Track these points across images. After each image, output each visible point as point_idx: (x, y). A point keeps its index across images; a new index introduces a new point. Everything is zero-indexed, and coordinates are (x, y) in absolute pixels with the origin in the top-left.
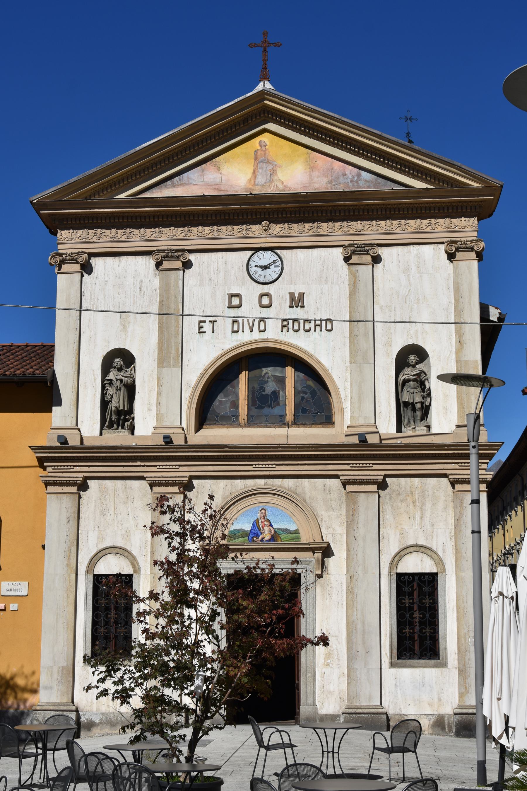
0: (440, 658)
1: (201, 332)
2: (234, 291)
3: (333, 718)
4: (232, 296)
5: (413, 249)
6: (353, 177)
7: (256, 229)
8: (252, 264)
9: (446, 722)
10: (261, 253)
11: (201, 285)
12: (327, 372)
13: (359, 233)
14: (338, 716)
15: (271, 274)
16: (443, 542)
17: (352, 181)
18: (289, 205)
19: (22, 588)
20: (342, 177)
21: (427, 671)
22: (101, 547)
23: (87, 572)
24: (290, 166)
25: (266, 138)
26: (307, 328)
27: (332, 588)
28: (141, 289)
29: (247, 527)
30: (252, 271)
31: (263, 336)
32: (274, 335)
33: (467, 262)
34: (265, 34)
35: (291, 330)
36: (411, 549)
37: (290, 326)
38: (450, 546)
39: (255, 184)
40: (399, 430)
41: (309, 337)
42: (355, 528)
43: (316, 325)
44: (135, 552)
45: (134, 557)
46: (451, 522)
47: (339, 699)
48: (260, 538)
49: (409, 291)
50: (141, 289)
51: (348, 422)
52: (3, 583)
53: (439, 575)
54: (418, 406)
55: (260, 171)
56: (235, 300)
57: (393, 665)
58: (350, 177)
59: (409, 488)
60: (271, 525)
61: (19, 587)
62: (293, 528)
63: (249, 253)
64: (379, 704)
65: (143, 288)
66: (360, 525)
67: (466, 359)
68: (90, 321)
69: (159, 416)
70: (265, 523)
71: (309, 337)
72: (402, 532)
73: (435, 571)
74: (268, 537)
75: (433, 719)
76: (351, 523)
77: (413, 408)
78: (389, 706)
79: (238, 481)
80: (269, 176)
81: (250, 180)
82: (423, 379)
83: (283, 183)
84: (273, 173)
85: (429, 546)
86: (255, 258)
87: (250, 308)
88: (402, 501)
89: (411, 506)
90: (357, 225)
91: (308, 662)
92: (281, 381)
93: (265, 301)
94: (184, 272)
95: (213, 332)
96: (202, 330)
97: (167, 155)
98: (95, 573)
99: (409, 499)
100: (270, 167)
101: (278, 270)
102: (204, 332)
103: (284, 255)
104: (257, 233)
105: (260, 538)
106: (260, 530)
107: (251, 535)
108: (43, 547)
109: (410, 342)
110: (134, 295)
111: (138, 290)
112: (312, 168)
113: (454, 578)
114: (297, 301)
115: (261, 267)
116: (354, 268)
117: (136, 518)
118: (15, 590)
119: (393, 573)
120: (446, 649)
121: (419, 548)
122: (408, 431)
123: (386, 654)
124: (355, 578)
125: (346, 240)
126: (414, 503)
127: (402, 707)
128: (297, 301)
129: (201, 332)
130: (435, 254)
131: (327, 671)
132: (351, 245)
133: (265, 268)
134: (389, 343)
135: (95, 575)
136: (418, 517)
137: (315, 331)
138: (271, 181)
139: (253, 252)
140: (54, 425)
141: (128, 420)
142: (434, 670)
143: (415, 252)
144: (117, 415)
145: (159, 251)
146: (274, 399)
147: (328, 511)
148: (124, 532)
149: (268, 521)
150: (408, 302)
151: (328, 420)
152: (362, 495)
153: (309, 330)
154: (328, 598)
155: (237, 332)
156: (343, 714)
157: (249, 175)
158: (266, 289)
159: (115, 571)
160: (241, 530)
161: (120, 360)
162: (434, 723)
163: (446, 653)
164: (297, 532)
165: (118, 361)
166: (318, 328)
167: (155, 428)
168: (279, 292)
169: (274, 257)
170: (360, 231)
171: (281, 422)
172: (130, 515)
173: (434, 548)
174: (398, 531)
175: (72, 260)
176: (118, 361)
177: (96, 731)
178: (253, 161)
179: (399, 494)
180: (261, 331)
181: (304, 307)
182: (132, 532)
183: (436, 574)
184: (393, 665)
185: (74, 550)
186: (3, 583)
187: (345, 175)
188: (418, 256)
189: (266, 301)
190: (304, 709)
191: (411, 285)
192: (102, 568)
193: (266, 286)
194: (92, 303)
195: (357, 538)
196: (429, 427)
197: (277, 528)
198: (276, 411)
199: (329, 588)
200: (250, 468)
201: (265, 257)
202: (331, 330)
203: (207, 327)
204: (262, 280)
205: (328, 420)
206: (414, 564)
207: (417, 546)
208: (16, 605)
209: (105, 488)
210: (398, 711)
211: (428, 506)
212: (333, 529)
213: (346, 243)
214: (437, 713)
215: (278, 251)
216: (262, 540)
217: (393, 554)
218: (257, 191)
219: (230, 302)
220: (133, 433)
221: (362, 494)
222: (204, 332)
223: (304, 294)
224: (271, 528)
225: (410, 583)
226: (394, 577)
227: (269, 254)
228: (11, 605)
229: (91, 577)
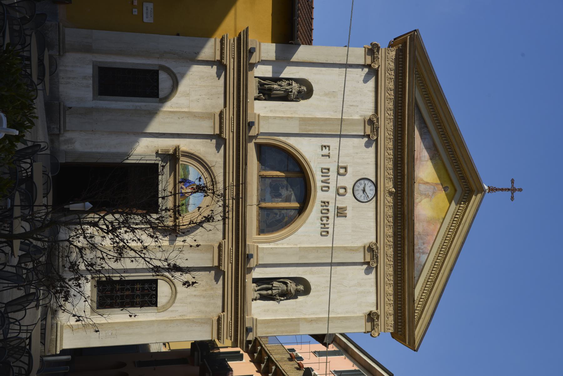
4: (345, 168)
5: (374, 289)
6: (422, 249)
8: (366, 182)
10: (373, 188)
13: (386, 254)
15: (359, 194)
17: (419, 248)
18: (406, 208)
19: (148, 19)
20: (422, 241)
28: (352, 106)
30: (362, 181)
31: (319, 190)
32: (319, 196)
34: (520, 190)
36: (173, 289)
37: (325, 207)
39: (419, 183)
40: (255, 281)
41: (317, 219)
43: (324, 224)
48: (183, 186)
50: (352, 106)
51: (260, 246)
55: (428, 187)
58: (422, 247)
63: (373, 179)
69: (267, 118)
71: (317, 219)
77: (269, 290)
79: (222, 171)
80: (424, 193)
81: (422, 180)
83: (420, 202)
84: (427, 196)
86: (370, 184)
90: (390, 251)
92: (288, 200)
96: (324, 148)
97: (442, 124)
100: (430, 194)
101: (362, 199)
102: (322, 150)
104: (387, 185)
105: (183, 186)
108: (178, 35)
109: (312, 287)
111: (352, 104)
112: (430, 221)
113: (153, 319)
114: (341, 212)
115: (364, 188)
116: (362, 250)
117: (198, 100)
118: (147, 13)
125: (381, 245)
128: (341, 212)
132: (377, 248)
133: (364, 191)
135: (158, 71)
138: (421, 194)
139: (375, 182)
140: (262, 44)
141: (264, 95)
143: (371, 290)
145: (378, 119)
146: (276, 195)
151: (261, 231)
153: (322, 220)
155: (322, 172)
157: (426, 180)
158: (350, 191)
160: (189, 174)
165: (304, 88)
166: (323, 226)
167: (259, 116)
168: (348, 201)
169: (371, 196)
170: (387, 253)
171: (261, 199)
173: (174, 305)
178: (435, 182)
180: (322, 187)
183: (156, 306)
187: (424, 244)
192: (163, 77)
198: (268, 196)
201: (371, 190)
202: (321, 235)
203: (326, 151)
204: (356, 188)
205: (261, 231)
208: (136, 13)
213: (378, 245)
215: (374, 199)
216: (182, 188)
218: (416, 185)
219: (342, 168)
220: (256, 99)
221: (212, 256)
222: (322, 150)
225: (151, 288)
227: (373, 192)
229: (156, 68)
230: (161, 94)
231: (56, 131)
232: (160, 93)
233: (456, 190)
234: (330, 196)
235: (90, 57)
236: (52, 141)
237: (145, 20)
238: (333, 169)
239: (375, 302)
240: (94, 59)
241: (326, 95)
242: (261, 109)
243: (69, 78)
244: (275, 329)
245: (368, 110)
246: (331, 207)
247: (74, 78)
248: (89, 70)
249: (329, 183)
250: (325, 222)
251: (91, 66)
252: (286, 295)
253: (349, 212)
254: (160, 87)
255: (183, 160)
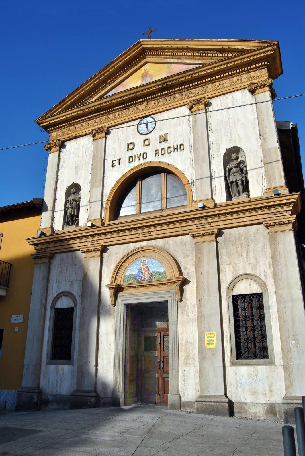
0: (269, 357)
1: (113, 165)
2: (130, 142)
3: (190, 404)
4: (129, 144)
5: (229, 95)
7: (141, 107)
9: (277, 409)
11: (114, 143)
12: (172, 166)
14: (193, 403)
16: (263, 269)
21: (259, 367)
22: (59, 292)
23: (51, 308)
24: (155, 71)
25: (147, 66)
26: (169, 151)
27: (188, 309)
28: (85, 152)
29: (135, 272)
31: (146, 161)
32: (152, 159)
33: (263, 93)
35: (160, 155)
37: (160, 152)
38: (270, 272)
41: (171, 156)
42: (201, 266)
43: (174, 149)
44: (75, 293)
45: (75, 297)
46: (269, 254)
47: (195, 390)
48: (143, 279)
49: (229, 118)
50: (85, 152)
52: (13, 316)
53: (264, 295)
54: (239, 182)
56: (130, 146)
57: (233, 364)
59: (237, 236)
60: (149, 270)
61: (19, 318)
62: (162, 270)
64: (223, 394)
65: (86, 151)
66: (205, 264)
67: (268, 148)
68: (62, 173)
70: (146, 269)
71: (171, 156)
72: (235, 267)
73: (260, 292)
74: (147, 278)
75: (267, 407)
76: (198, 264)
78: (231, 396)
79: (131, 244)
82: (242, 167)
85: (255, 274)
87: (139, 149)
88: (233, 245)
89: (240, 248)
91: (174, 362)
93: (147, 143)
94: (106, 138)
95: (119, 165)
96: (114, 165)
98: (56, 308)
99: (238, 243)
102: (115, 166)
103: (156, 117)
106: (142, 274)
107: (138, 278)
109: (232, 146)
110: (82, 156)
114: (164, 139)
118: (17, 320)
119: (230, 295)
120: (273, 350)
121: (246, 276)
122: (235, 200)
123: (227, 355)
124: (202, 301)
126: (241, 245)
127: (242, 397)
128: (164, 139)
129: (113, 165)
130: (243, 96)
131: (186, 368)
134: (218, 149)
136: (245, 255)
137: (174, 152)
142: (264, 367)
143: (231, 97)
144: (71, 218)
147: (184, 257)
148: (70, 283)
149: (148, 267)
150: (228, 124)
152: (205, 244)
154: (186, 316)
156: (196, 401)
158: (147, 137)
159: (66, 306)
161: (74, 189)
162: (267, 410)
163: (273, 354)
164: (164, 273)
166: (176, 150)
168: (154, 137)
170: (195, 93)
172: (74, 272)
173: (258, 275)
174: (231, 266)
175: (55, 146)
176: (73, 190)
177: (50, 407)
179: (230, 241)
181: (167, 141)
182: (74, 282)
183: (261, 294)
184: (233, 364)
185: (44, 295)
186: (13, 316)
188: (233, 98)
189: (146, 143)
190: (171, 398)
191: (229, 115)
193: (147, 135)
194: (63, 164)
195: (203, 273)
196: (249, 196)
197: (152, 272)
199: (186, 309)
200: (136, 236)
203: (116, 163)
206: (244, 288)
207: (245, 274)
209: (63, 259)
210: (238, 400)
211: (252, 245)
212: (188, 269)
214: (269, 402)
215: (152, 116)
217: (229, 282)
219: (128, 147)
222: (115, 166)
223: (167, 134)
224: (149, 272)
226: (231, 299)
228: (15, 328)
229: (53, 310)
230: (71, 305)
231: (93, 400)
232: (70, 307)
233: (146, 63)
234: (150, 151)
235: (43, 367)
236: (105, 405)
237: (21, 321)
238: (130, 153)
239: (241, 91)
240: (45, 363)
241: (77, 173)
242: (83, 221)
243: (57, 385)
244: (276, 170)
245: (87, 140)
246: (159, 147)
247: (57, 381)
248: (52, 367)
249: (140, 154)
250: (172, 150)
251: (50, 366)
252: (242, 169)
253: (163, 133)
254: (66, 306)
255: (120, 281)
